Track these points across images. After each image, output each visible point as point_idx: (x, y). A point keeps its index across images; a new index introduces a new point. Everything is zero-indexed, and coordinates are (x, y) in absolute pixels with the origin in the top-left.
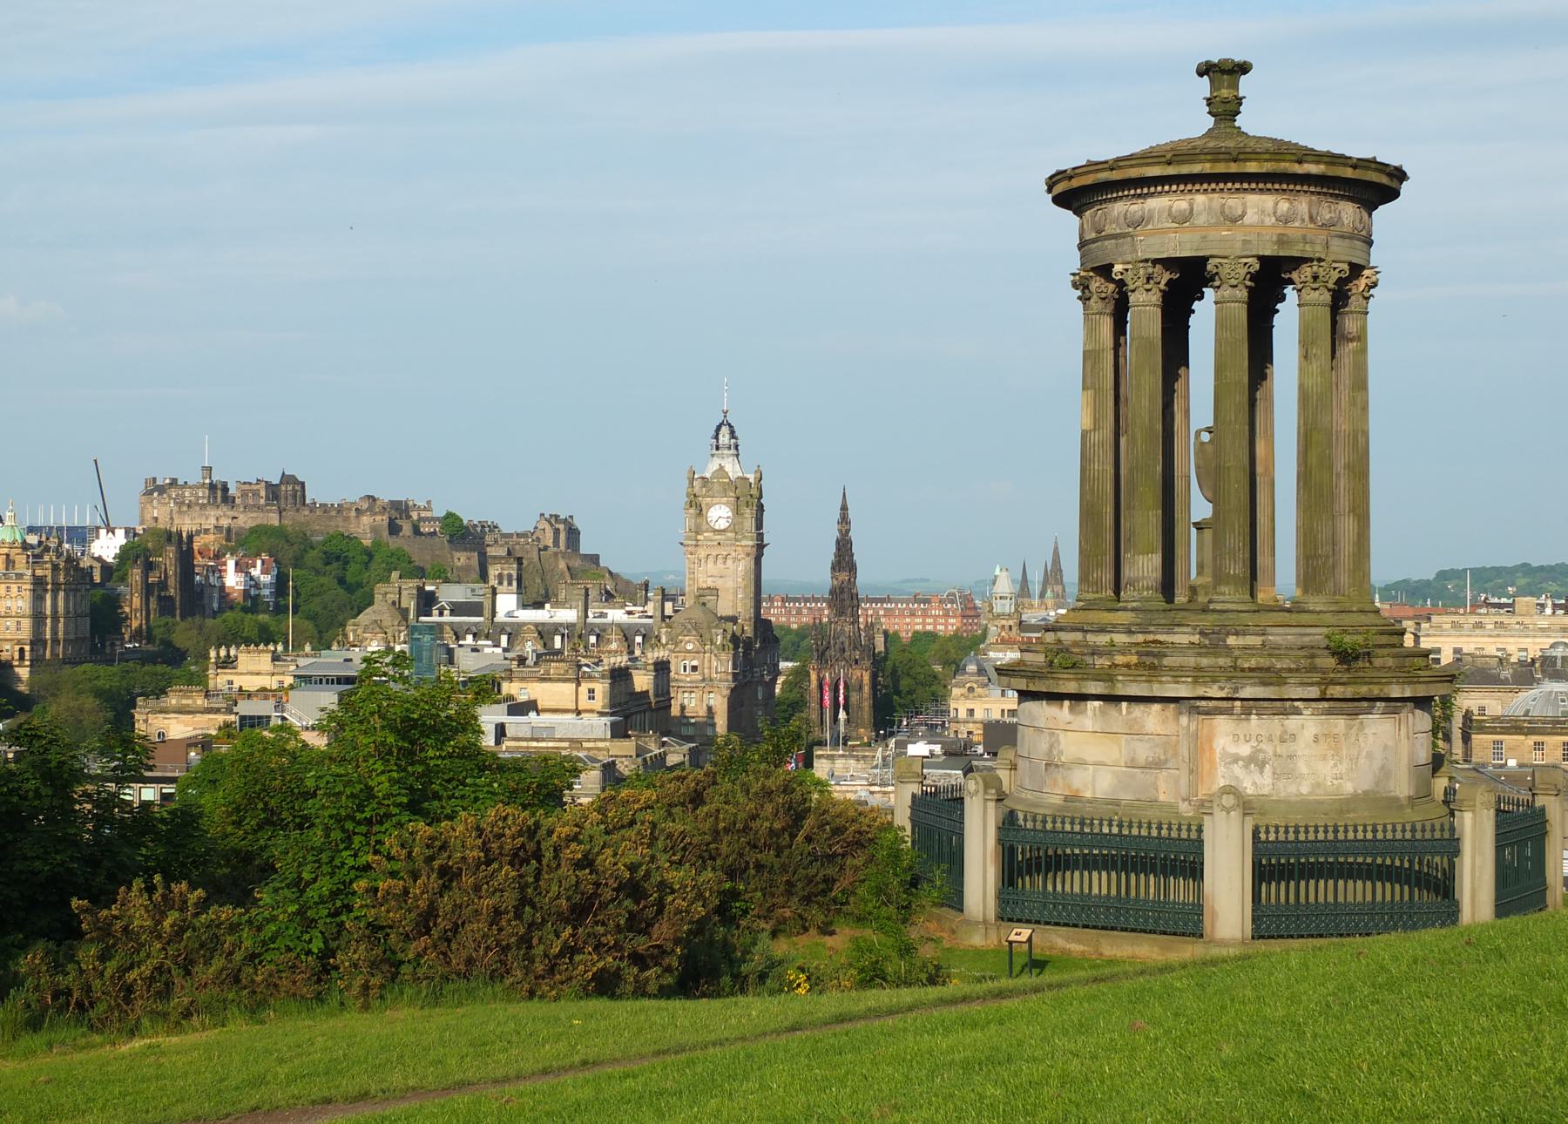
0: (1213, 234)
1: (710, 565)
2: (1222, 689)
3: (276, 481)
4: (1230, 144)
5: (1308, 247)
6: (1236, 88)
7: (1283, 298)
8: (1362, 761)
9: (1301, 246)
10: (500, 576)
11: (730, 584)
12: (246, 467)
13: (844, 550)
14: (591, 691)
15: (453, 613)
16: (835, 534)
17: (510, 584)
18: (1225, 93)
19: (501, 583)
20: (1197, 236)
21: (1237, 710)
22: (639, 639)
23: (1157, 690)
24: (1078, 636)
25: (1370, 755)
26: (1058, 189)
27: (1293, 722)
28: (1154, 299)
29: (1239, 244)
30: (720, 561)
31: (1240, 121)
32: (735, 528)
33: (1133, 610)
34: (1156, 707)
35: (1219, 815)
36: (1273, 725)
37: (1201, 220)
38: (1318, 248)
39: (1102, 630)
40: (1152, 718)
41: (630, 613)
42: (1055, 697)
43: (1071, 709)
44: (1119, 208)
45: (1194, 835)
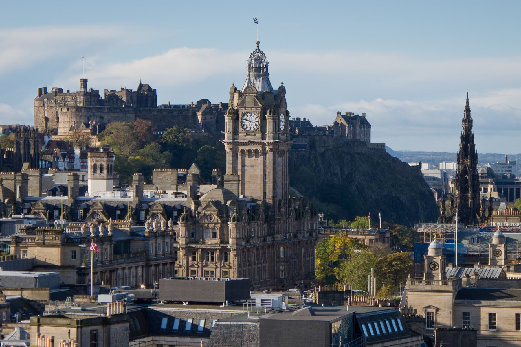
3: (135, 89)
10: (95, 165)
11: (259, 172)
12: (116, 77)
17: (101, 171)
19: (95, 171)
22: (175, 213)
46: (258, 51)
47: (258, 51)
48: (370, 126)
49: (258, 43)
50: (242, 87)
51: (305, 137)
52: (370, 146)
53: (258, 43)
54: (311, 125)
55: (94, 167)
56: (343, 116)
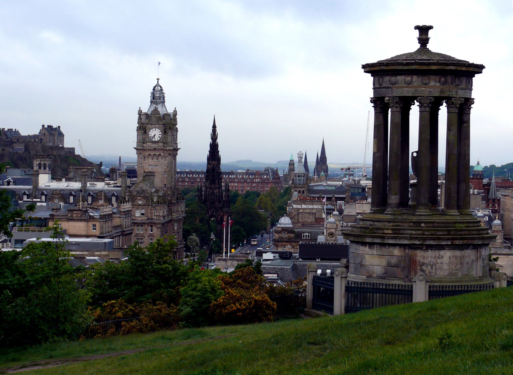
0: (419, 89)
1: (150, 160)
2: (419, 241)
4: (425, 57)
5: (450, 93)
6: (427, 34)
7: (442, 105)
8: (465, 265)
9: (448, 93)
13: (214, 148)
14: (94, 225)
15: (15, 183)
16: (210, 141)
17: (45, 168)
18: (424, 37)
19: (40, 168)
20: (413, 89)
21: (424, 248)
23: (398, 242)
24: (372, 223)
25: (467, 263)
26: (367, 69)
27: (442, 253)
28: (398, 109)
29: (428, 92)
30: (155, 158)
31: (429, 46)
32: (163, 141)
33: (390, 214)
34: (397, 248)
35: (418, 282)
36: (436, 253)
37: (415, 84)
38: (454, 93)
39: (379, 221)
40: (397, 252)
41: (108, 184)
42: (364, 244)
43: (369, 248)
44: (387, 79)
45: (410, 289)
46: (158, 85)
47: (158, 85)
48: (63, 136)
49: (158, 79)
50: (145, 110)
51: (22, 143)
52: (66, 150)
53: (158, 79)
54: (20, 134)
55: (40, 166)
56: (45, 128)
